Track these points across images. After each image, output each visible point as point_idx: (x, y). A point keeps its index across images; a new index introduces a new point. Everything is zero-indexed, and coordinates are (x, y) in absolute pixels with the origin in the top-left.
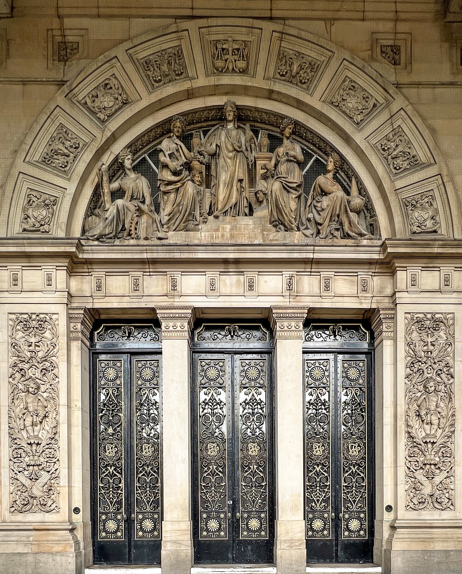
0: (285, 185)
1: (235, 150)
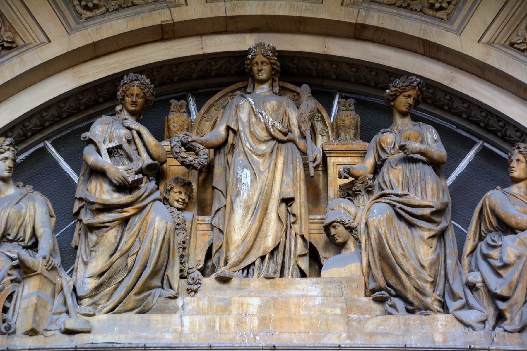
0: (399, 211)
1: (274, 138)
